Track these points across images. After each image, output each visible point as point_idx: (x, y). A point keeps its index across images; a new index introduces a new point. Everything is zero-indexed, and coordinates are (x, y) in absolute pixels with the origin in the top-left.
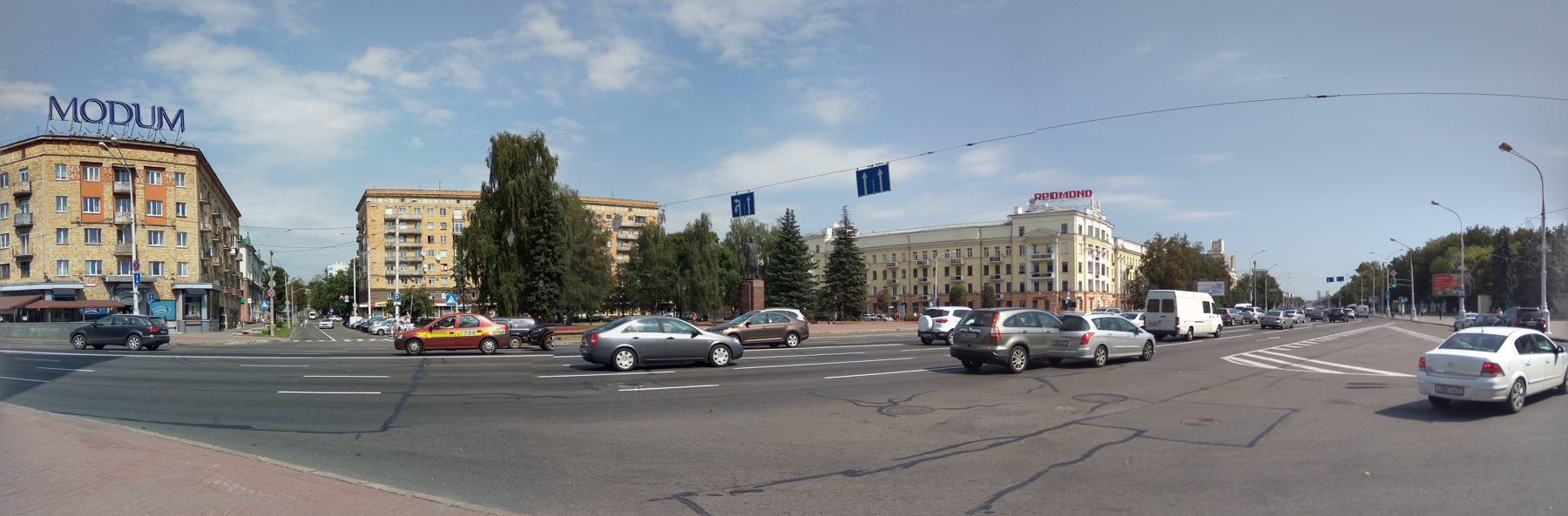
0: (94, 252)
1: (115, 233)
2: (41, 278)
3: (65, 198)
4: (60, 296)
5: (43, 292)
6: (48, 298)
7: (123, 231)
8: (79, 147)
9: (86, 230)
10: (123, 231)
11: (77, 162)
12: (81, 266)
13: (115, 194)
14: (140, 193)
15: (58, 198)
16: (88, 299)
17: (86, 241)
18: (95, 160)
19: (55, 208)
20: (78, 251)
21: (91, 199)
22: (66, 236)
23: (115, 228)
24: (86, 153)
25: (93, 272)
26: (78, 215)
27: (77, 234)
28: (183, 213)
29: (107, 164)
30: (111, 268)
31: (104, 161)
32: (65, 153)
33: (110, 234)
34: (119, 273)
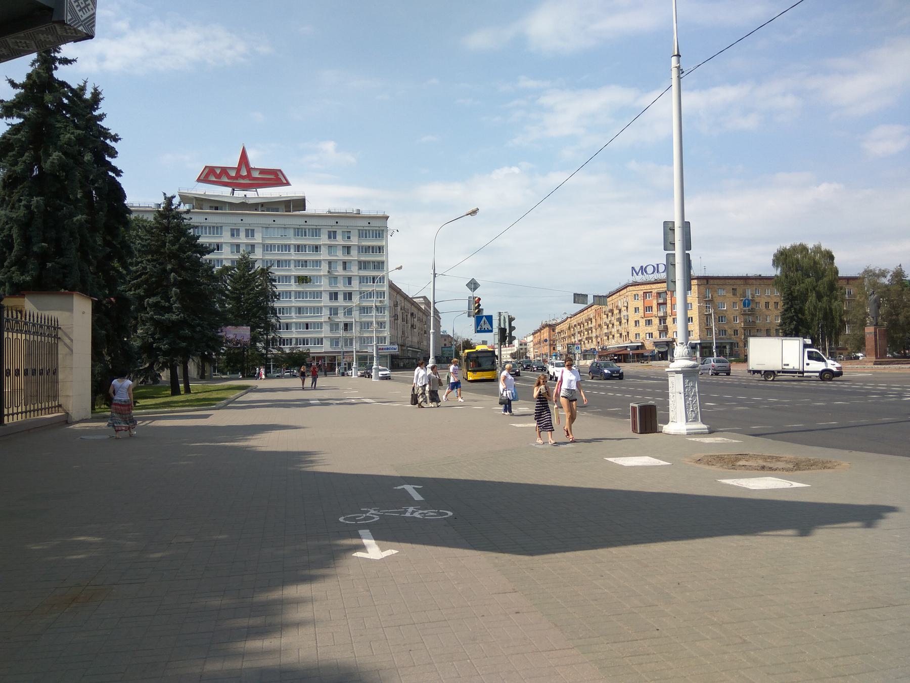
0: (649, 329)
1: (658, 320)
2: (630, 341)
3: (638, 308)
4: (632, 348)
5: (627, 347)
6: (629, 349)
7: (663, 319)
8: (643, 286)
9: (646, 320)
10: (663, 319)
11: (642, 292)
12: (644, 335)
13: (657, 304)
14: (669, 302)
15: (636, 308)
16: (647, 349)
17: (646, 325)
18: (649, 291)
19: (634, 312)
20: (643, 329)
21: (649, 307)
22: (639, 323)
23: (658, 318)
24: (645, 288)
25: (650, 337)
26: (642, 315)
27: (642, 322)
28: (691, 307)
29: (654, 291)
30: (656, 334)
31: (653, 291)
32: (638, 289)
33: (656, 321)
34: (660, 337)
